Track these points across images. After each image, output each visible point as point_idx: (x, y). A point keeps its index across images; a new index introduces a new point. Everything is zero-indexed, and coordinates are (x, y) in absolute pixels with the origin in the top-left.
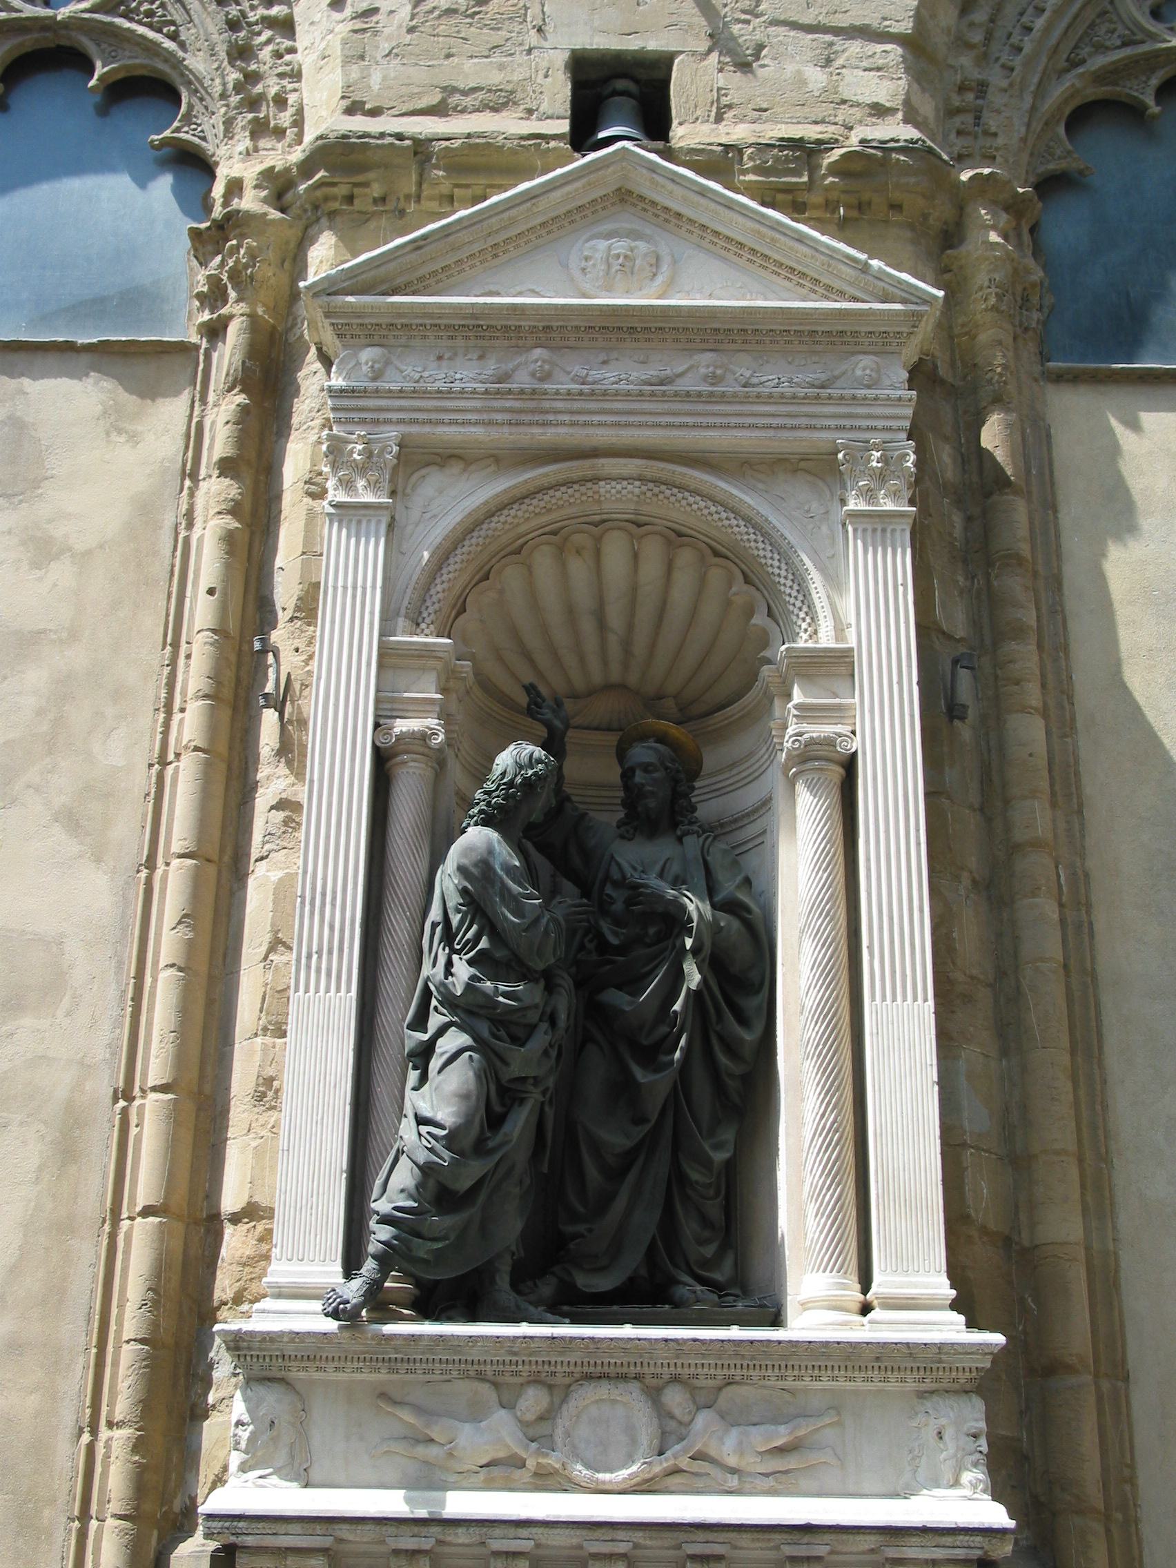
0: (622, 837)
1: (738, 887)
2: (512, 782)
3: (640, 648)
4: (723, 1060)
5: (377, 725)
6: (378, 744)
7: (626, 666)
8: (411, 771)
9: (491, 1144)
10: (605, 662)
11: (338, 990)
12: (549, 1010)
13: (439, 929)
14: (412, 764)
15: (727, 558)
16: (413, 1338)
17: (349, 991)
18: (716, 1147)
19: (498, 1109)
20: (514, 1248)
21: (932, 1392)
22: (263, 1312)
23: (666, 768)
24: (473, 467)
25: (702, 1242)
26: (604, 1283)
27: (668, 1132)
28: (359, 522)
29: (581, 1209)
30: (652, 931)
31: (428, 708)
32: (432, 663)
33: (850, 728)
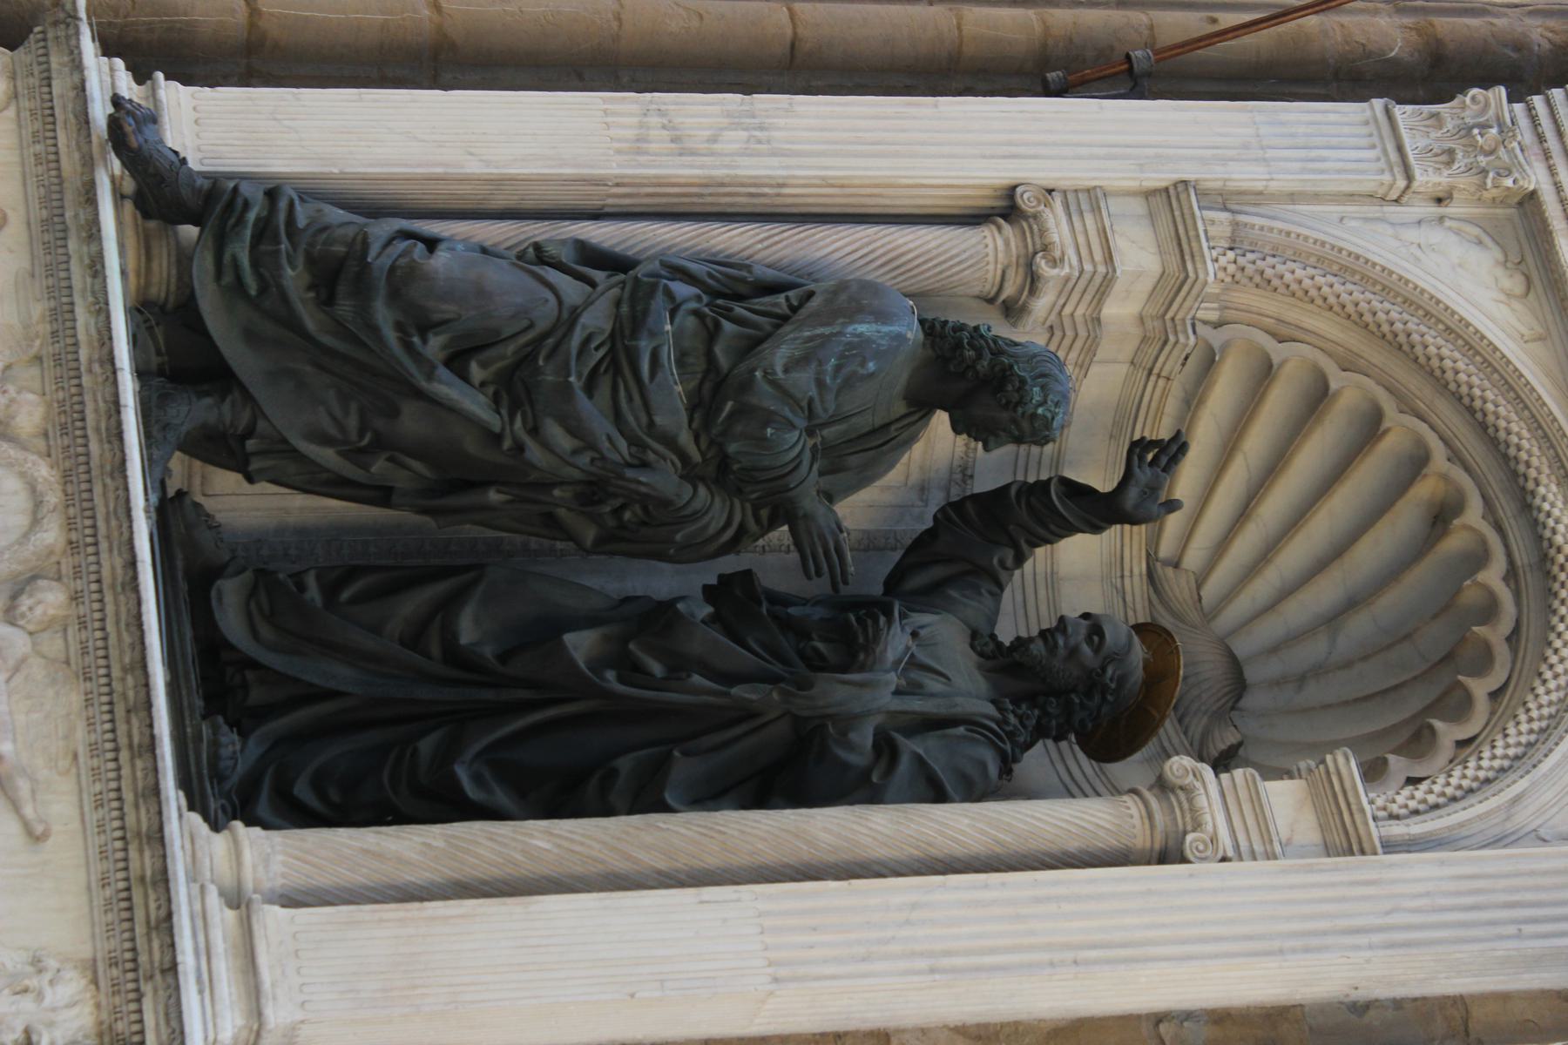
0: (974, 635)
1: (920, 761)
2: (1001, 352)
3: (1314, 693)
4: (625, 764)
5: (1050, 191)
6: (1019, 190)
7: (1278, 683)
8: (989, 241)
9: (416, 340)
10: (1274, 649)
11: (619, 152)
12: (651, 457)
13: (745, 274)
14: (1000, 242)
15: (1493, 713)
16: (96, 266)
17: (619, 166)
18: (478, 779)
19: (476, 372)
20: (261, 425)
21: (95, 981)
22: (112, 70)
23: (1104, 669)
24: (1517, 305)
25: (318, 785)
26: (231, 621)
27: (489, 695)
28: (1373, 147)
29: (345, 595)
30: (820, 645)
31: (1098, 256)
32: (1174, 261)
33: (1230, 853)
